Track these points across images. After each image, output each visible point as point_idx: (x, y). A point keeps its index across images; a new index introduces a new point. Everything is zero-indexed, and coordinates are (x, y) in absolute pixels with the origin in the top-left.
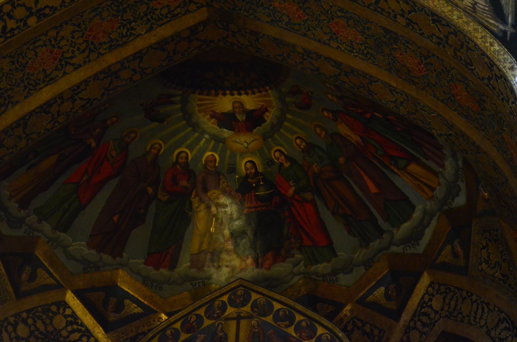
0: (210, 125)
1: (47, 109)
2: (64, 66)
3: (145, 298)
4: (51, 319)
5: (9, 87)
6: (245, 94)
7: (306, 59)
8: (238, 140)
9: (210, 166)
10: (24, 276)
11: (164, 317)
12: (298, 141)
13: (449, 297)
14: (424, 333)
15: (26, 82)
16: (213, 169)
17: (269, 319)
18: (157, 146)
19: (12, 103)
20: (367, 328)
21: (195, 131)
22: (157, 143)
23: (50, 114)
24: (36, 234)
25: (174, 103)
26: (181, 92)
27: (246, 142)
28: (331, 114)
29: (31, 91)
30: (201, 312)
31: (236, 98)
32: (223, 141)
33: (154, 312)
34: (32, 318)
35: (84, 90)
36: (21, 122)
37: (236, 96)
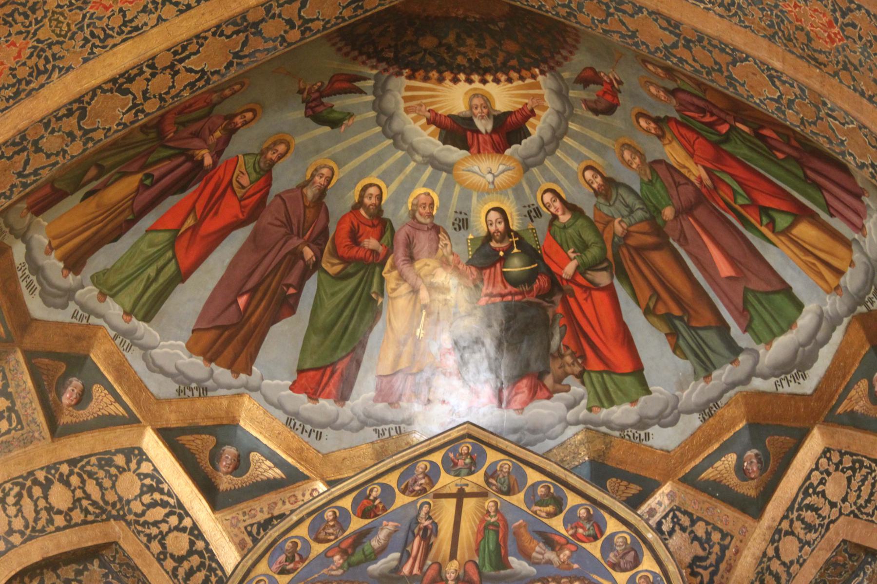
0: (427, 139)
1: (125, 86)
2: (160, 6)
3: (288, 450)
4: (114, 479)
5: (55, 39)
6: (494, 81)
7: (612, 15)
8: (476, 169)
9: (421, 214)
10: (67, 398)
11: (321, 487)
12: (589, 174)
13: (858, 477)
14: (808, 543)
15: (87, 32)
16: (428, 221)
17: (518, 499)
18: (325, 171)
19: (60, 69)
20: (700, 530)
21: (396, 145)
22: (325, 166)
23: (131, 96)
24: (93, 320)
25: (360, 91)
26: (375, 72)
27: (490, 172)
28: (653, 125)
29: (95, 50)
30: (392, 480)
31: (475, 89)
32: (448, 168)
33: (306, 478)
34: (79, 475)
35: (195, 54)
36: (75, 106)
37: (477, 85)
